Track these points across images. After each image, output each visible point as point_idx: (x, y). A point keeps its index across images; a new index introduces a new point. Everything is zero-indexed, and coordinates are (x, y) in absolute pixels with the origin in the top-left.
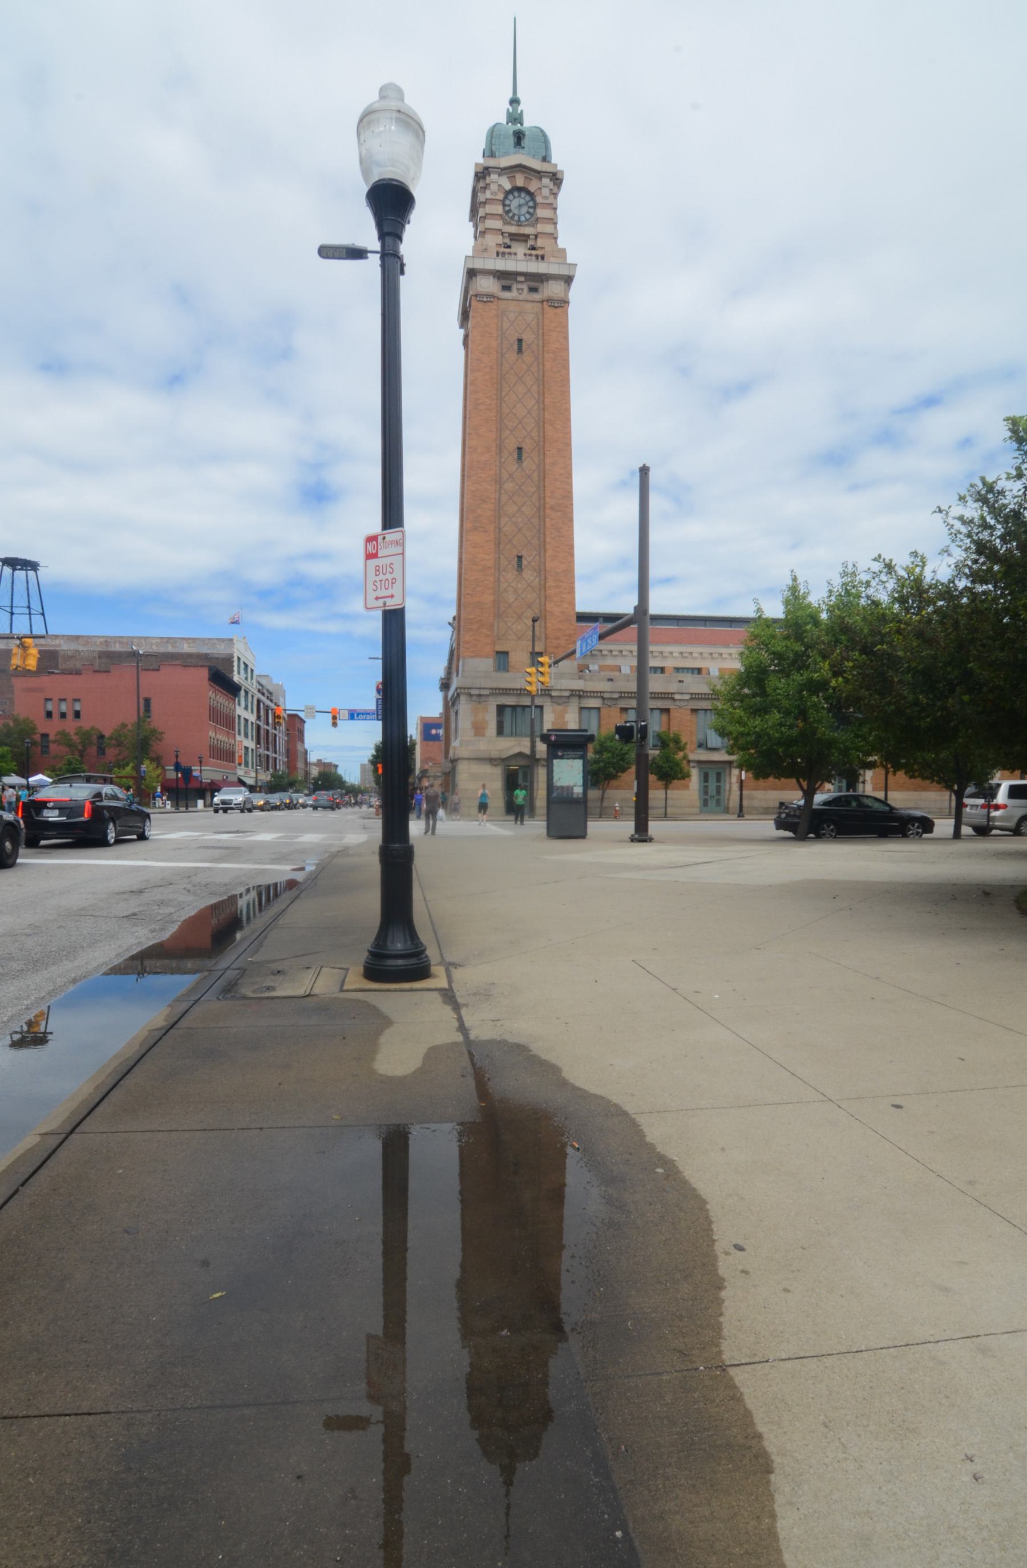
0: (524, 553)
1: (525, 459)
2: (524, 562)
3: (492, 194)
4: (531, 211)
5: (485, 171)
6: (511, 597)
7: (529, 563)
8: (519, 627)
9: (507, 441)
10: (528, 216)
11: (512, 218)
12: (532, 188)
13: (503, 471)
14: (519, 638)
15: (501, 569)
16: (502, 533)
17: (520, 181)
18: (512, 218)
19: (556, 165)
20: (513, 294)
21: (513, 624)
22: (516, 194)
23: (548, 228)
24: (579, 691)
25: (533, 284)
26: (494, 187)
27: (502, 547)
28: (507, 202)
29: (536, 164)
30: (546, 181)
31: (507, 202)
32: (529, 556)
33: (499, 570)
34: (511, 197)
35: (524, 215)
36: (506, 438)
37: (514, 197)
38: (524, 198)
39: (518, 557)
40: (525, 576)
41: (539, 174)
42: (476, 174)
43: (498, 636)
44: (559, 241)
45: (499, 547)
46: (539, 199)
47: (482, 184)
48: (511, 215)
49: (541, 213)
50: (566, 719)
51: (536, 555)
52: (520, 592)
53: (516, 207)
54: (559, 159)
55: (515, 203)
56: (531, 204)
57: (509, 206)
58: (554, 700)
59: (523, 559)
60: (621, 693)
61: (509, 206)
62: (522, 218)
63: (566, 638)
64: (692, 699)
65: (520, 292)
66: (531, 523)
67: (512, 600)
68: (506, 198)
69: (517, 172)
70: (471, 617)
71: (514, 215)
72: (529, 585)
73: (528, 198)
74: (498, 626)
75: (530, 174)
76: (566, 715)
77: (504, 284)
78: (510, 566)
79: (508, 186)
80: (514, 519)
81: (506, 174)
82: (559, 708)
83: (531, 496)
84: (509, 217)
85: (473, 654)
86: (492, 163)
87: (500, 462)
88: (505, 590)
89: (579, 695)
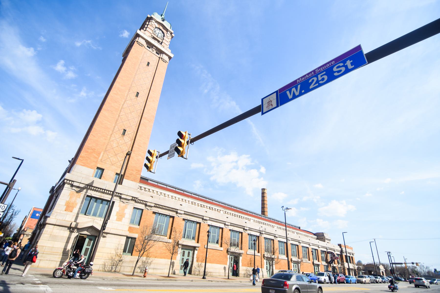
0: (127, 130)
1: (139, 97)
2: (126, 133)
5: (151, 18)
6: (115, 145)
7: (128, 134)
8: (114, 160)
9: (133, 87)
13: (128, 96)
14: (113, 165)
15: (114, 131)
16: (119, 118)
20: (151, 50)
21: (111, 157)
24: (136, 198)
27: (118, 123)
32: (129, 131)
33: (113, 131)
36: (133, 87)
39: (124, 130)
40: (124, 138)
43: (101, 160)
45: (116, 122)
48: (155, 33)
50: (125, 212)
51: (133, 132)
52: (120, 144)
58: (121, 200)
59: (126, 131)
60: (155, 204)
63: (136, 171)
64: (184, 214)
66: (134, 120)
67: (115, 146)
70: (90, 146)
72: (125, 143)
74: (103, 156)
76: (126, 210)
77: (148, 46)
78: (119, 132)
80: (127, 115)
82: (123, 205)
83: (137, 110)
85: (83, 164)
87: (128, 93)
88: (113, 141)
89: (134, 199)
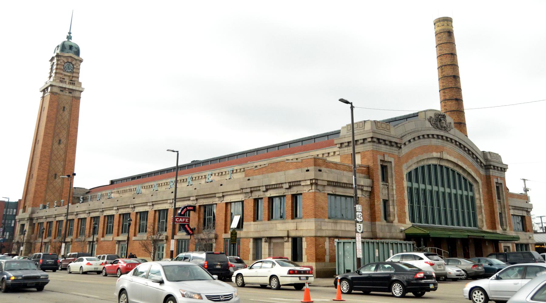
3: (61, 62)
4: (72, 69)
10: (71, 70)
11: (66, 70)
12: (74, 63)
17: (70, 61)
18: (66, 70)
19: (81, 58)
22: (68, 63)
25: (71, 91)
26: (62, 61)
28: (65, 65)
29: (76, 57)
41: (76, 60)
46: (75, 66)
48: (65, 69)
49: (75, 70)
54: (82, 56)
56: (72, 67)
73: (71, 65)
79: (66, 61)
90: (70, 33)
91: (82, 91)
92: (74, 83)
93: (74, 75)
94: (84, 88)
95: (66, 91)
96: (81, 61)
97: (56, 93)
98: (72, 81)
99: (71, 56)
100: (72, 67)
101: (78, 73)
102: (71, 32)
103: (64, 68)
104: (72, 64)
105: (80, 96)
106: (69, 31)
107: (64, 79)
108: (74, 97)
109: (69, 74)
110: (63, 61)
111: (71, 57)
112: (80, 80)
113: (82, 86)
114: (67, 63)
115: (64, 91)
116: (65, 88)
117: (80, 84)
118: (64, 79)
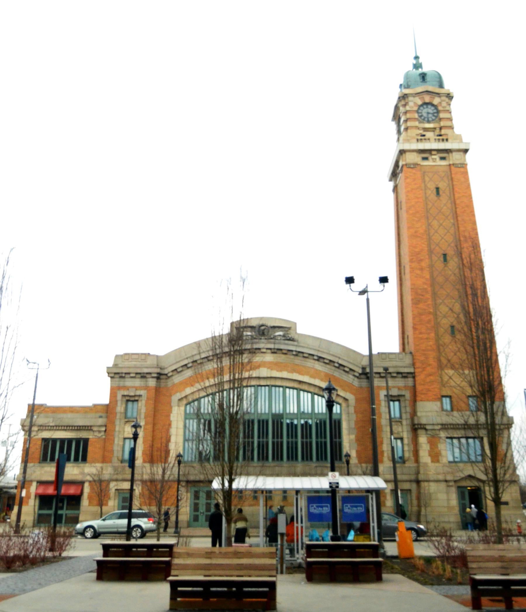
3: (410, 107)
4: (436, 115)
10: (434, 118)
11: (424, 119)
17: (427, 99)
18: (424, 119)
22: (425, 106)
23: (448, 123)
26: (411, 104)
28: (420, 111)
29: (438, 90)
30: (444, 98)
31: (420, 111)
34: (422, 108)
35: (431, 118)
37: (424, 108)
38: (431, 110)
42: (399, 98)
44: (455, 130)
46: (440, 108)
47: (403, 102)
48: (423, 118)
49: (442, 115)
53: (425, 112)
55: (425, 111)
56: (435, 111)
57: (421, 113)
61: (421, 113)
62: (430, 119)
65: (434, 160)
68: (419, 109)
69: (424, 94)
71: (425, 118)
73: (433, 108)
75: (433, 95)
79: (420, 102)
81: (418, 96)
84: (421, 119)
86: (407, 91)
90: (417, 58)
91: (466, 151)
92: (447, 140)
93: (442, 124)
94: (469, 143)
95: (434, 157)
96: (450, 97)
97: (416, 165)
98: (440, 135)
99: (427, 91)
100: (435, 111)
101: (450, 119)
102: (418, 55)
103: (421, 116)
104: (433, 105)
105: (465, 160)
106: (414, 55)
107: (424, 136)
108: (453, 164)
109: (431, 125)
110: (415, 103)
111: (428, 92)
112: (457, 130)
113: (464, 140)
114: (422, 105)
115: (430, 158)
116: (430, 151)
117: (459, 138)
118: (424, 136)
